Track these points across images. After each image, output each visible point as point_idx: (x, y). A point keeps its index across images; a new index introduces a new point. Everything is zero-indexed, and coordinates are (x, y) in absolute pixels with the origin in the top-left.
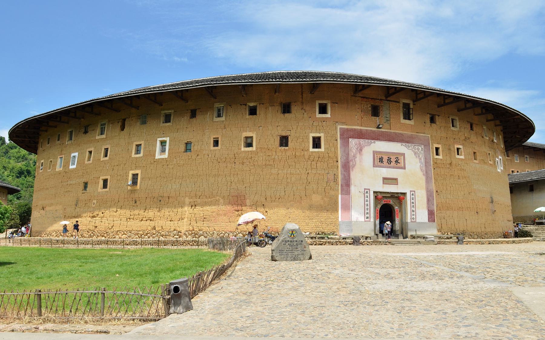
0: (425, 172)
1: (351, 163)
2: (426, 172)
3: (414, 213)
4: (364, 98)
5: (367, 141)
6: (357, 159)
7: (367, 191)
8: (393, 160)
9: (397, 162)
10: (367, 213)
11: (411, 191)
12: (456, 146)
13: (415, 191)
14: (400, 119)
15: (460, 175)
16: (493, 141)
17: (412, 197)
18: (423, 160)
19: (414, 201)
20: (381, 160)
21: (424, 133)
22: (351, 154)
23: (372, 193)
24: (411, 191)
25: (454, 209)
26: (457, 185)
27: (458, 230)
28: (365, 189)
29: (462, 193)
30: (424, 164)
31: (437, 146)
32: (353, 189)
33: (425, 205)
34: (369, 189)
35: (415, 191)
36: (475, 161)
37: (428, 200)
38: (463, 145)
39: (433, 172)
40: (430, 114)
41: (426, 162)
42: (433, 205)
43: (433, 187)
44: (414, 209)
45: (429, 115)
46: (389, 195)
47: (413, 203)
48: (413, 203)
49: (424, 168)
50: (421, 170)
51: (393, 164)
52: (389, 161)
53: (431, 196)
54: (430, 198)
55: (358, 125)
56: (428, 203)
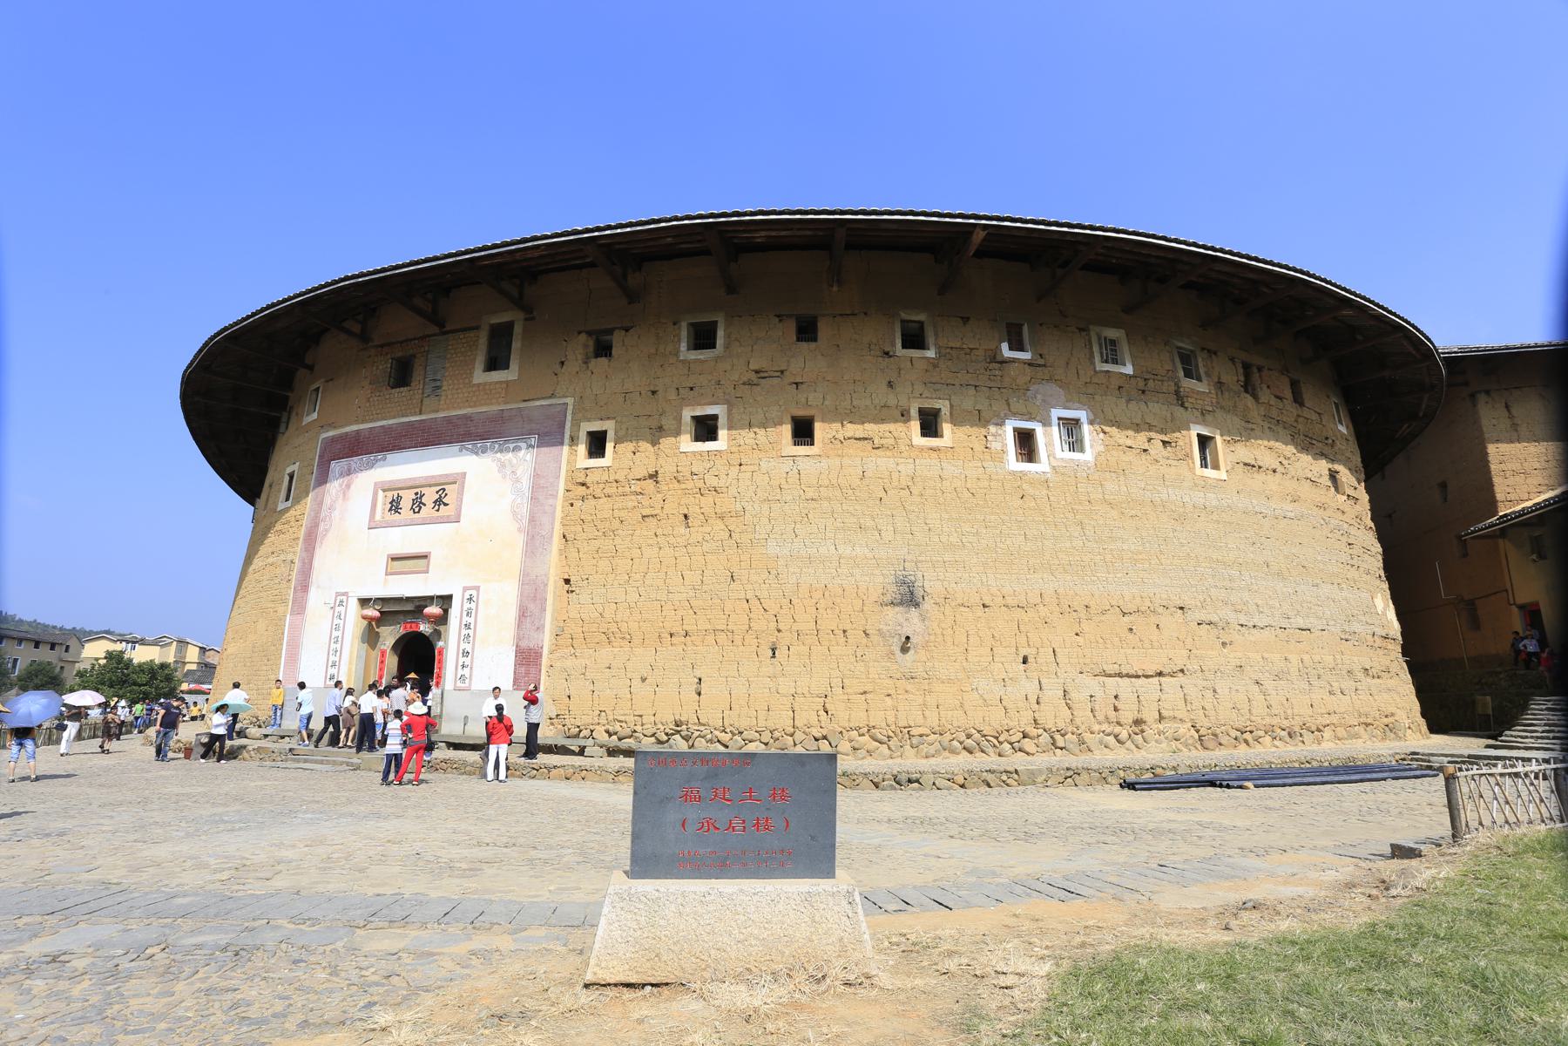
0: (525, 521)
1: (322, 527)
2: (532, 520)
3: (467, 661)
4: (389, 344)
5: (365, 458)
6: (336, 514)
7: (341, 599)
8: (430, 496)
9: (439, 502)
10: (334, 665)
11: (465, 589)
12: (688, 414)
13: (477, 588)
14: (472, 373)
15: (693, 511)
16: (995, 359)
17: (467, 605)
18: (526, 483)
19: (471, 620)
20: (395, 506)
21: (552, 396)
22: (327, 501)
23: (353, 604)
24: (465, 589)
25: (636, 641)
26: (668, 551)
27: (648, 719)
28: (338, 594)
29: (692, 577)
30: (527, 494)
31: (596, 426)
32: (318, 599)
33: (509, 633)
34: (345, 594)
35: (477, 588)
36: (802, 450)
37: (523, 614)
38: (728, 402)
39: (559, 514)
40: (589, 333)
41: (536, 488)
42: (540, 629)
43: (552, 566)
44: (468, 648)
45: (583, 337)
46: (409, 607)
47: (468, 626)
48: (468, 626)
49: (524, 511)
50: (514, 513)
51: (426, 511)
52: (418, 503)
53: (534, 599)
54: (531, 606)
55: (357, 422)
56: (519, 625)
